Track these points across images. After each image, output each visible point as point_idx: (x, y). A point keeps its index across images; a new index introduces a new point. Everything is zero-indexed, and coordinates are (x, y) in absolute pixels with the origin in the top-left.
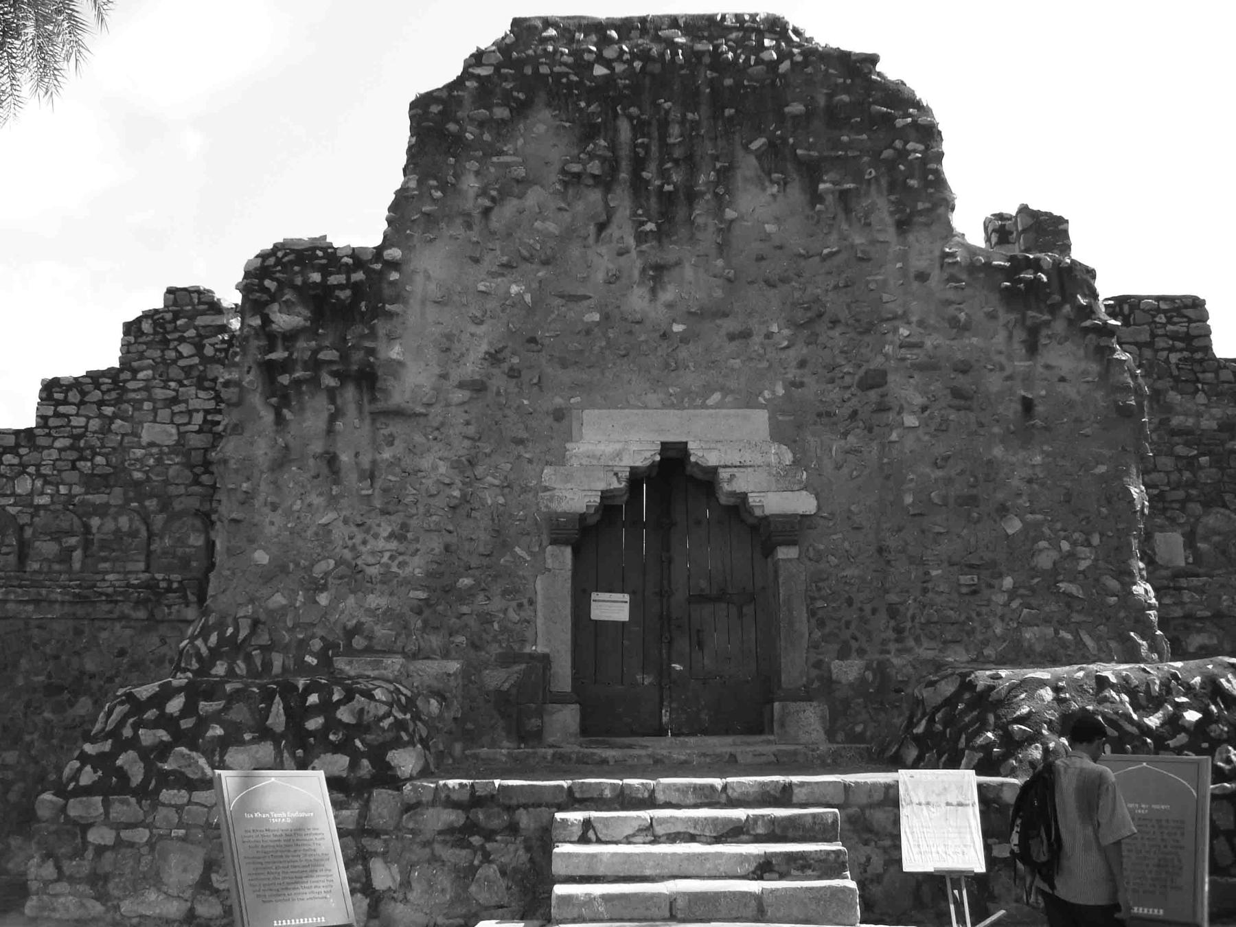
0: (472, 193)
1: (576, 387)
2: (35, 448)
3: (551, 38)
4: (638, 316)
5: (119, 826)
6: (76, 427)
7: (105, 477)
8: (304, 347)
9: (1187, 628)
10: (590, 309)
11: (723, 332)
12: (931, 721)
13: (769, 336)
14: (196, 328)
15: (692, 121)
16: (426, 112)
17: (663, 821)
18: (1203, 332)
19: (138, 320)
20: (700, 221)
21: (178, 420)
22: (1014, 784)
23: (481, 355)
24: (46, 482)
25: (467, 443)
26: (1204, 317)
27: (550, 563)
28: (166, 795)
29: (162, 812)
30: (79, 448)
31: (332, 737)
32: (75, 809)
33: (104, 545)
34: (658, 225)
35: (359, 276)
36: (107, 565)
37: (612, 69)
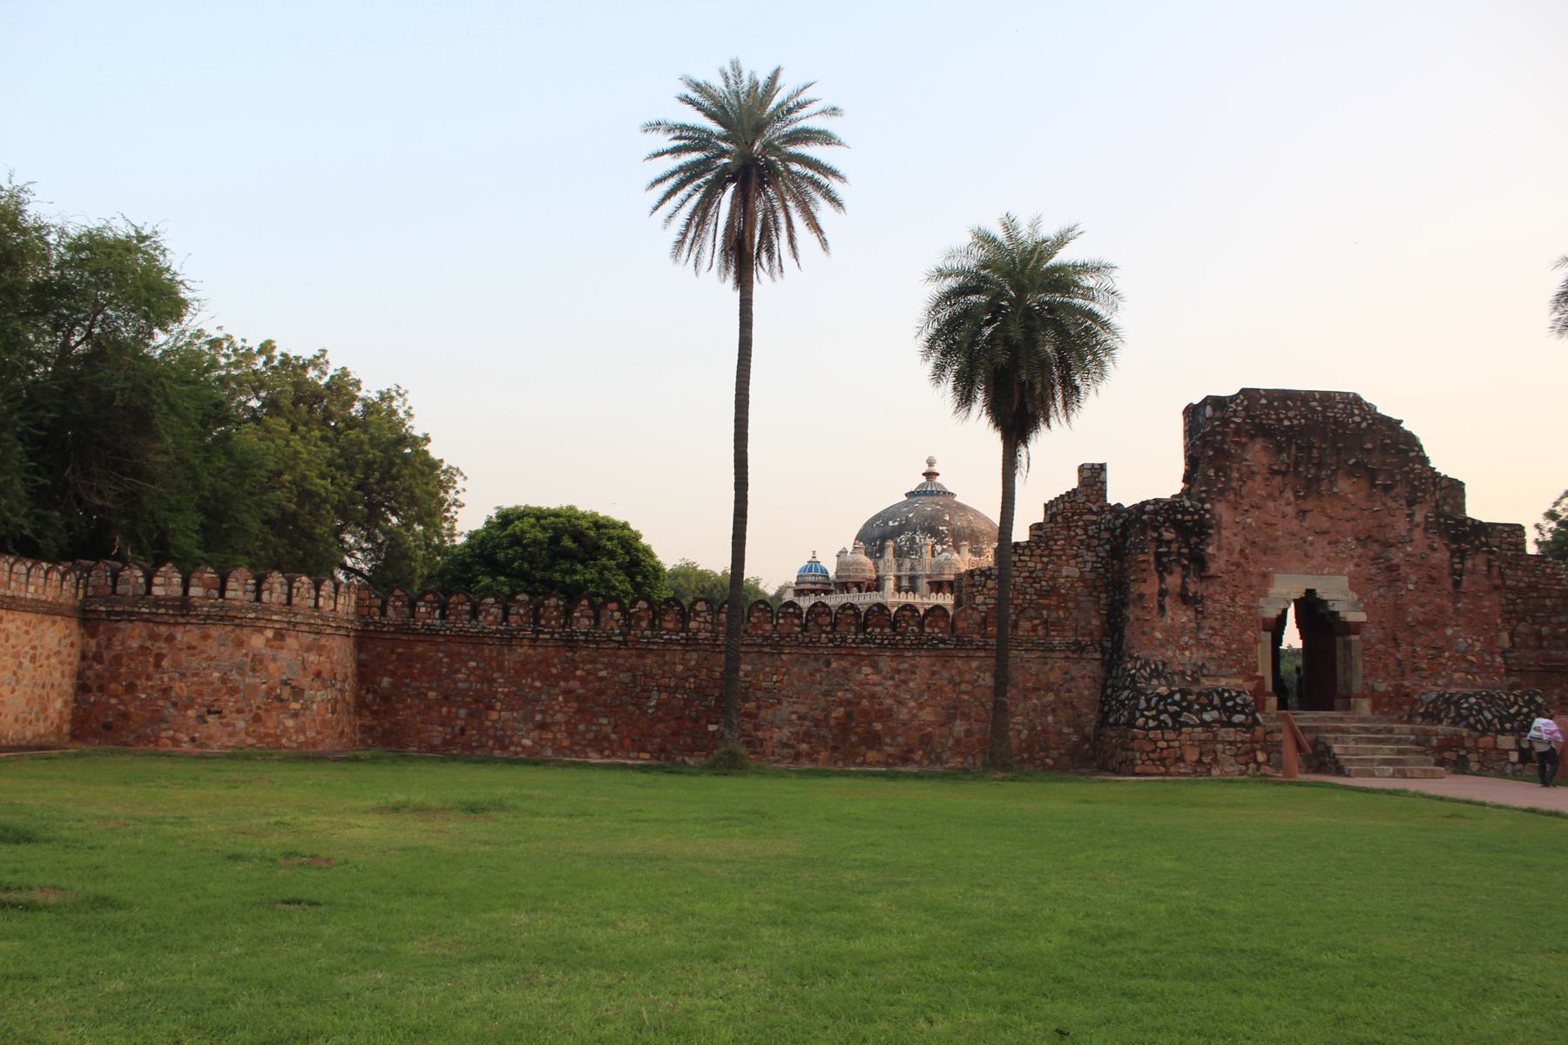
5: (1167, 741)
7: (1047, 591)
8: (1174, 547)
10: (1278, 530)
12: (1427, 708)
13: (1347, 543)
21: (1079, 565)
28: (1184, 729)
29: (1182, 737)
32: (1151, 735)
35: (1196, 517)
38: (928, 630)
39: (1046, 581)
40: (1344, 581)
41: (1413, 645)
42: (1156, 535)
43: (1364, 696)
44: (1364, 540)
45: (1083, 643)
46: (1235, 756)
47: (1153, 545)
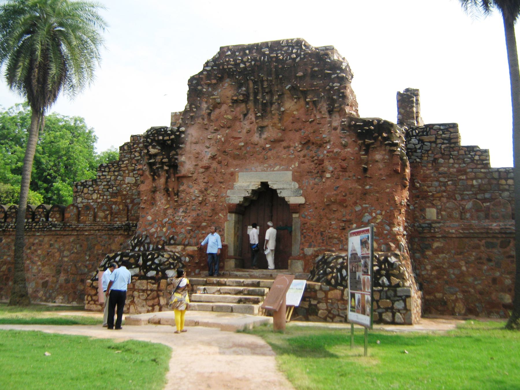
0: (204, 109)
1: (237, 166)
2: (97, 185)
3: (228, 55)
4: (256, 143)
7: (116, 193)
8: (159, 158)
9: (433, 240)
10: (241, 142)
11: (282, 146)
14: (139, 147)
15: (270, 80)
16: (192, 83)
17: (222, 289)
18: (455, 137)
19: (123, 146)
20: (273, 112)
22: (318, 285)
23: (208, 158)
24: (100, 196)
25: (204, 184)
26: (457, 132)
27: (229, 218)
30: (109, 185)
31: (153, 267)
33: (116, 213)
34: (262, 114)
35: (173, 137)
36: (117, 219)
37: (245, 65)
38: (50, 219)
39: (116, 187)
40: (289, 175)
41: (330, 220)
43: (299, 259)
44: (307, 143)
45: (131, 225)
46: (146, 300)
47: (146, 157)
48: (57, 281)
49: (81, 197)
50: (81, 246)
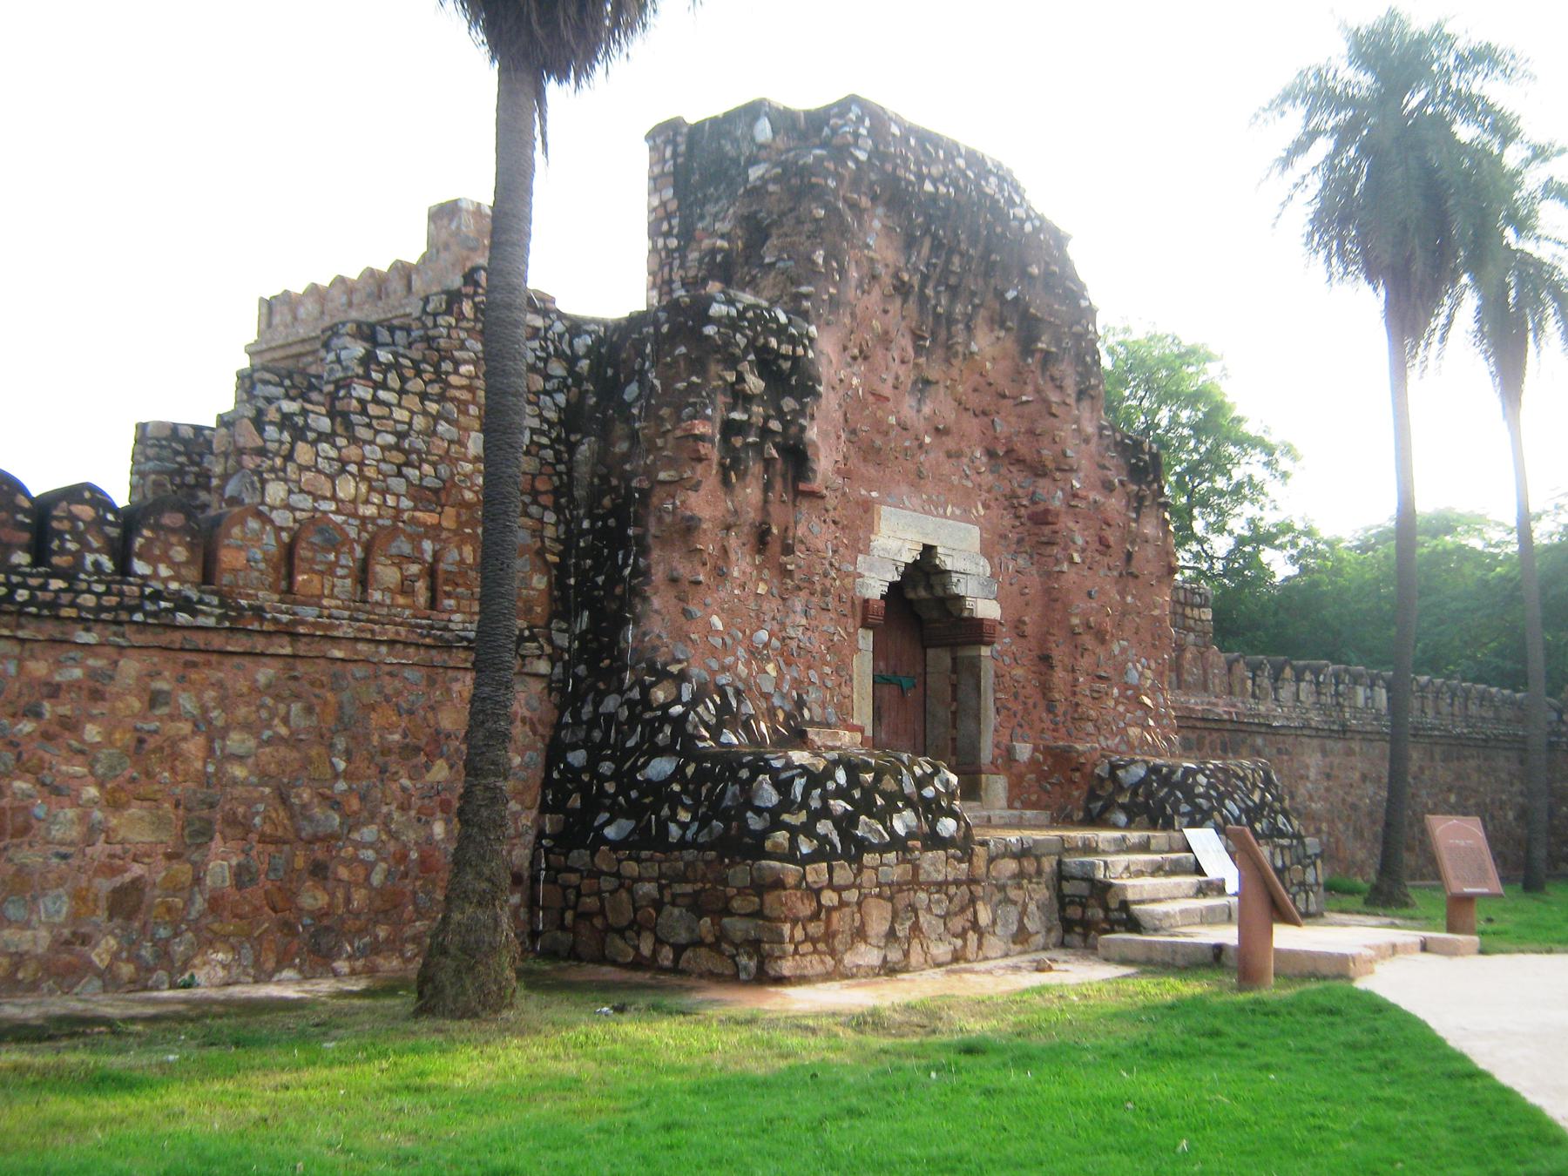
2: (354, 440)
6: (397, 422)
7: (436, 491)
24: (371, 489)
28: (868, 858)
38: (140, 567)
42: (731, 377)
44: (1001, 456)
47: (721, 400)
48: (198, 880)
49: (286, 481)
50: (309, 710)
